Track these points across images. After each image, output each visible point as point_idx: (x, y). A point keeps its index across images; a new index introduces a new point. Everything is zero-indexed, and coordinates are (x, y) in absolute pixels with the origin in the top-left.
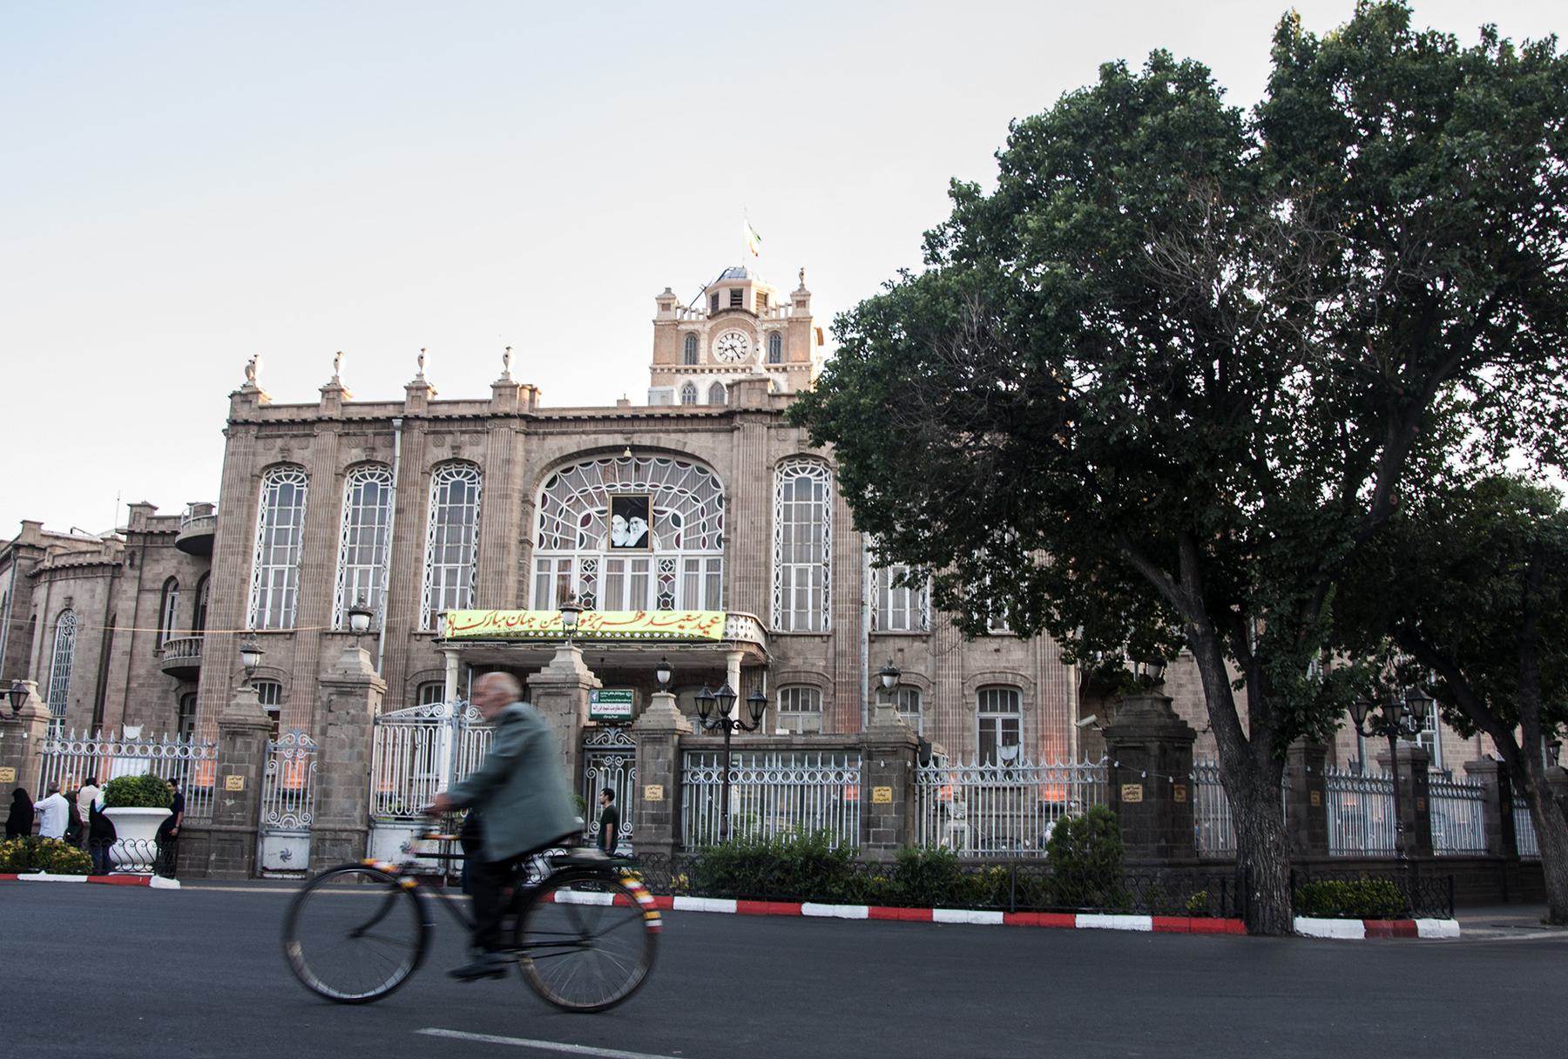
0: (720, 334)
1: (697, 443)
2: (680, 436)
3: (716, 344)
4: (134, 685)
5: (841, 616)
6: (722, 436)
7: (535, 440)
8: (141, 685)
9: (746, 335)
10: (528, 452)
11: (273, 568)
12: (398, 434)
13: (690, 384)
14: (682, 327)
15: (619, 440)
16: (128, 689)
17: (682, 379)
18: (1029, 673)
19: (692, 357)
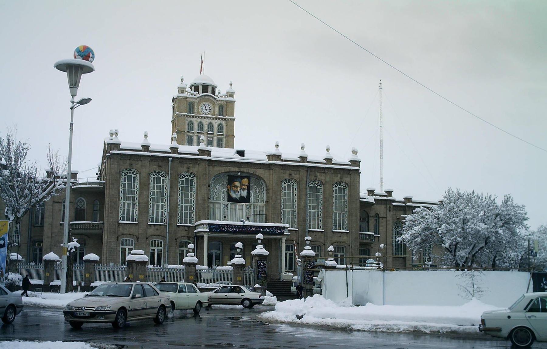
0: (202, 104)
1: (260, 172)
2: (255, 170)
3: (200, 107)
4: (53, 235)
5: (301, 225)
6: (266, 171)
7: (211, 168)
8: (56, 236)
9: (211, 105)
10: (209, 171)
11: (126, 202)
12: (170, 163)
13: (191, 121)
14: (188, 99)
15: (237, 169)
16: (51, 237)
17: (189, 119)
18: (348, 242)
19: (191, 110)
